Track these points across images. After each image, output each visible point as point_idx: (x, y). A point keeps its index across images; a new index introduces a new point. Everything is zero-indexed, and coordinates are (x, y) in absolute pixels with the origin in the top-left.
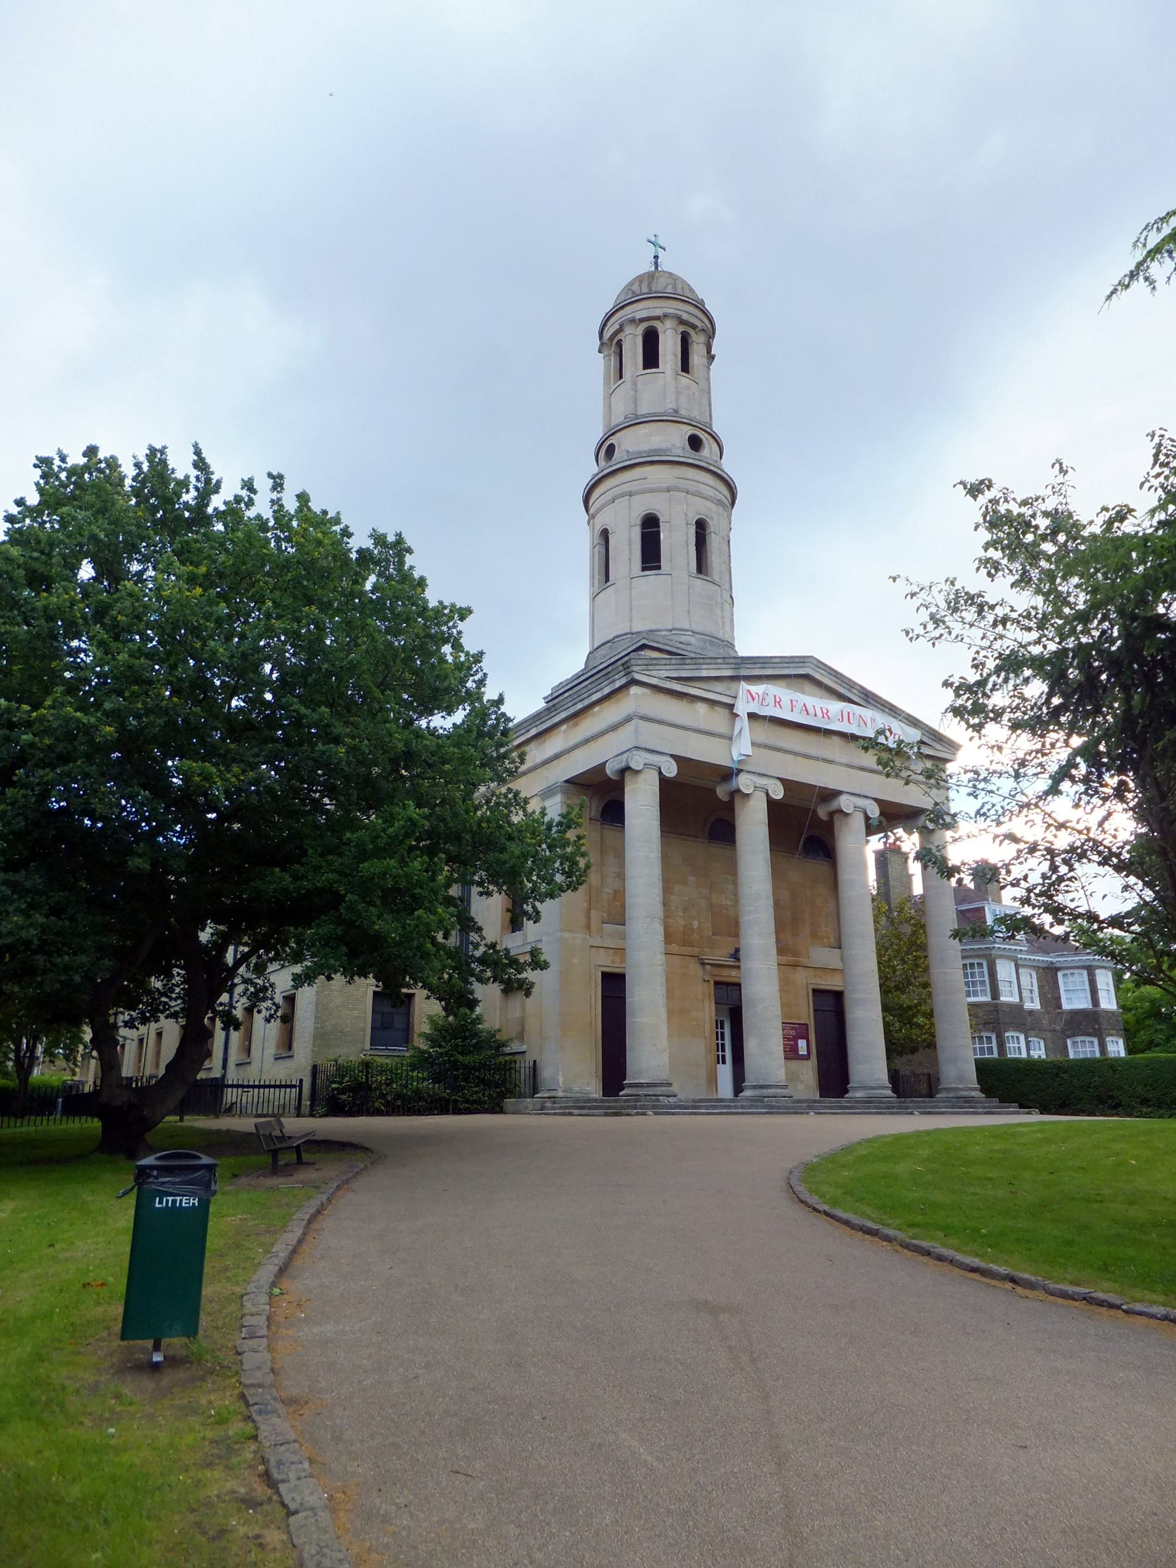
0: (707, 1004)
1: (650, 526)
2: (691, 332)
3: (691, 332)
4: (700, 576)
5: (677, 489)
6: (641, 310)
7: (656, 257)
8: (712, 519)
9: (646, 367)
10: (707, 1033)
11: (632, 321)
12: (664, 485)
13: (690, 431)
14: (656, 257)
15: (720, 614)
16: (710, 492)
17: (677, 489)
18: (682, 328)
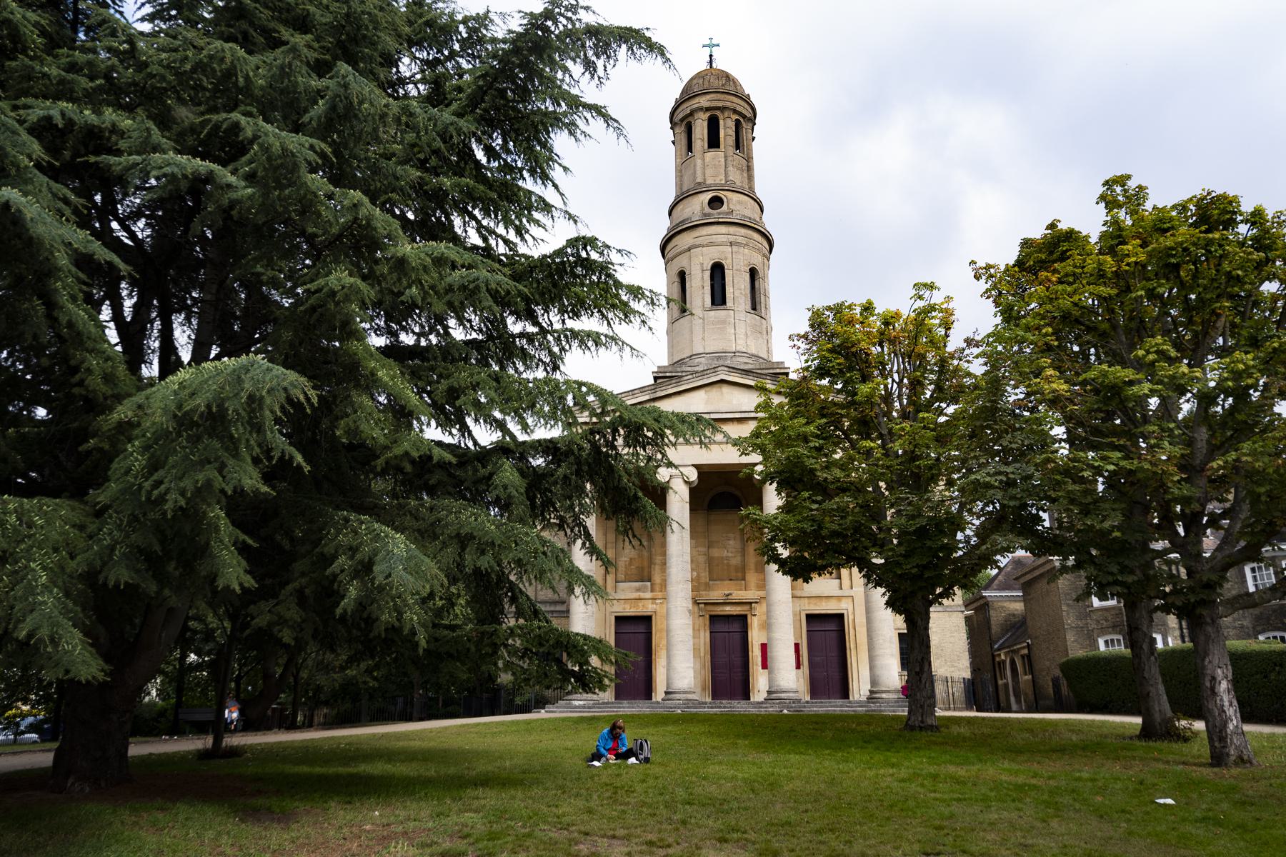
0: (702, 633)
1: (718, 271)
2: (717, 113)
3: (717, 113)
4: (714, 307)
5: (695, 247)
6: (703, 101)
7: (711, 56)
8: (726, 259)
9: (710, 146)
10: (702, 654)
11: (701, 109)
12: (687, 247)
13: (709, 196)
14: (711, 56)
15: (733, 331)
16: (723, 239)
17: (695, 247)
18: (708, 114)
